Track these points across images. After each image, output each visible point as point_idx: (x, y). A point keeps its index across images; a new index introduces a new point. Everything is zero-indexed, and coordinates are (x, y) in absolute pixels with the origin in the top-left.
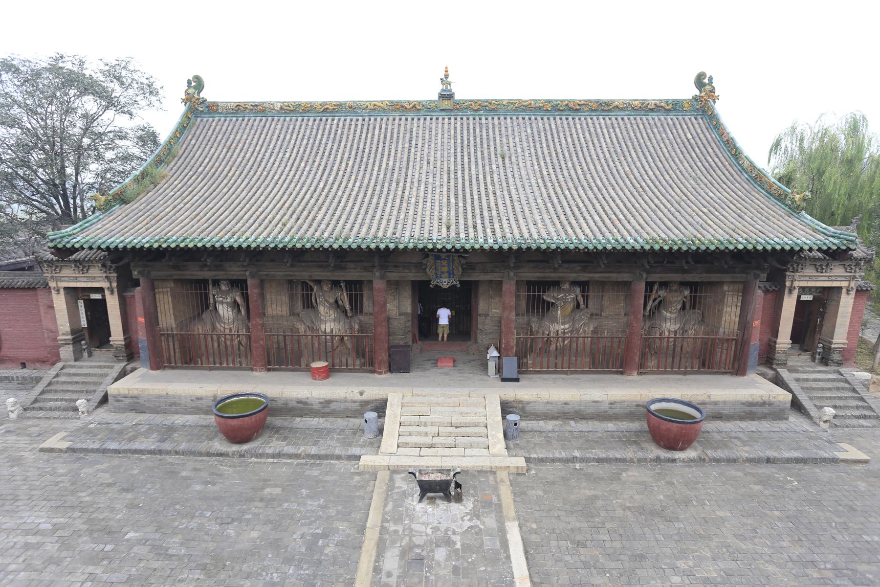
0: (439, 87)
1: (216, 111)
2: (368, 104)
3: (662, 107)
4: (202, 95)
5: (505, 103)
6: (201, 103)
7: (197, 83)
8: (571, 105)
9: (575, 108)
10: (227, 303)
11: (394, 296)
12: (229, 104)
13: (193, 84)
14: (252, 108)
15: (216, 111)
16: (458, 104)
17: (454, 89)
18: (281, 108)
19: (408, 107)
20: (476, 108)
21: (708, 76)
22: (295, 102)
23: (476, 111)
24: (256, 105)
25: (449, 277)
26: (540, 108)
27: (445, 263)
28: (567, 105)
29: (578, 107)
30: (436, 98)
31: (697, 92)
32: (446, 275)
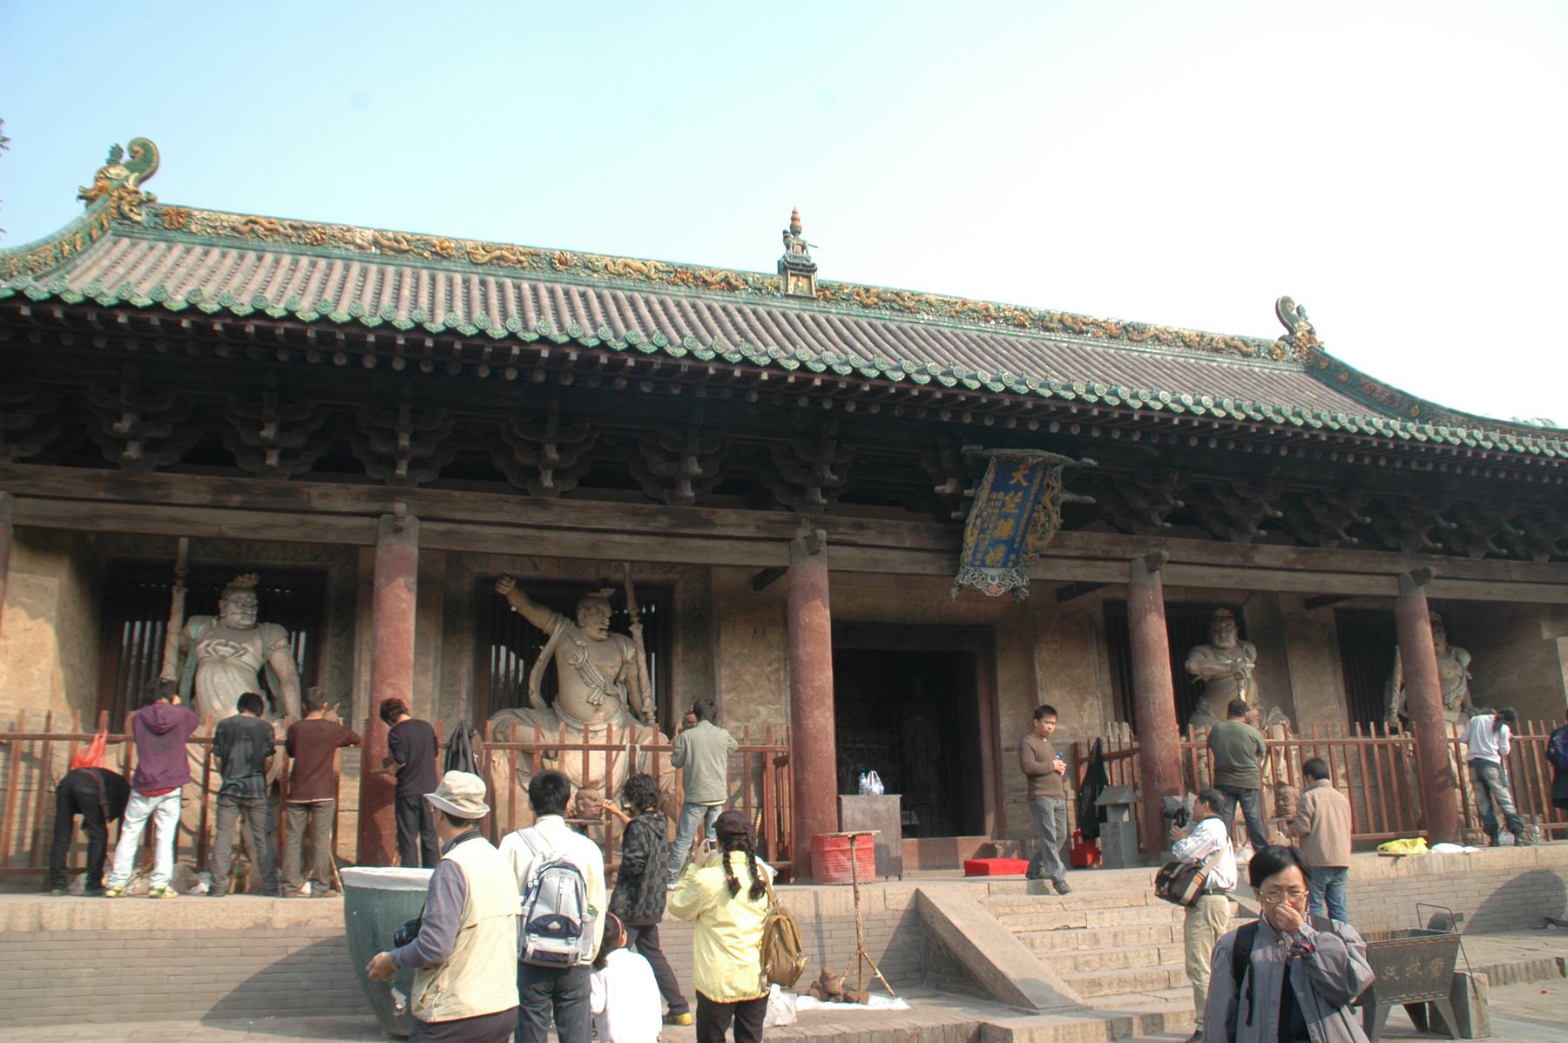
0: (780, 251)
1: (182, 228)
2: (607, 261)
3: (1236, 347)
4: (144, 188)
5: (932, 299)
6: (141, 203)
7: (144, 159)
8: (1069, 322)
9: (1077, 328)
10: (241, 669)
11: (778, 681)
12: (223, 217)
13: (126, 157)
14: (290, 231)
15: (182, 228)
16: (827, 288)
17: (814, 256)
18: (376, 243)
19: (709, 279)
20: (869, 302)
21: (1296, 307)
22: (413, 234)
23: (866, 306)
24: (304, 228)
25: (1004, 565)
26: (1006, 319)
27: (1012, 501)
28: (1061, 321)
29: (1084, 328)
30: (774, 270)
31: (1287, 333)
32: (1000, 552)
